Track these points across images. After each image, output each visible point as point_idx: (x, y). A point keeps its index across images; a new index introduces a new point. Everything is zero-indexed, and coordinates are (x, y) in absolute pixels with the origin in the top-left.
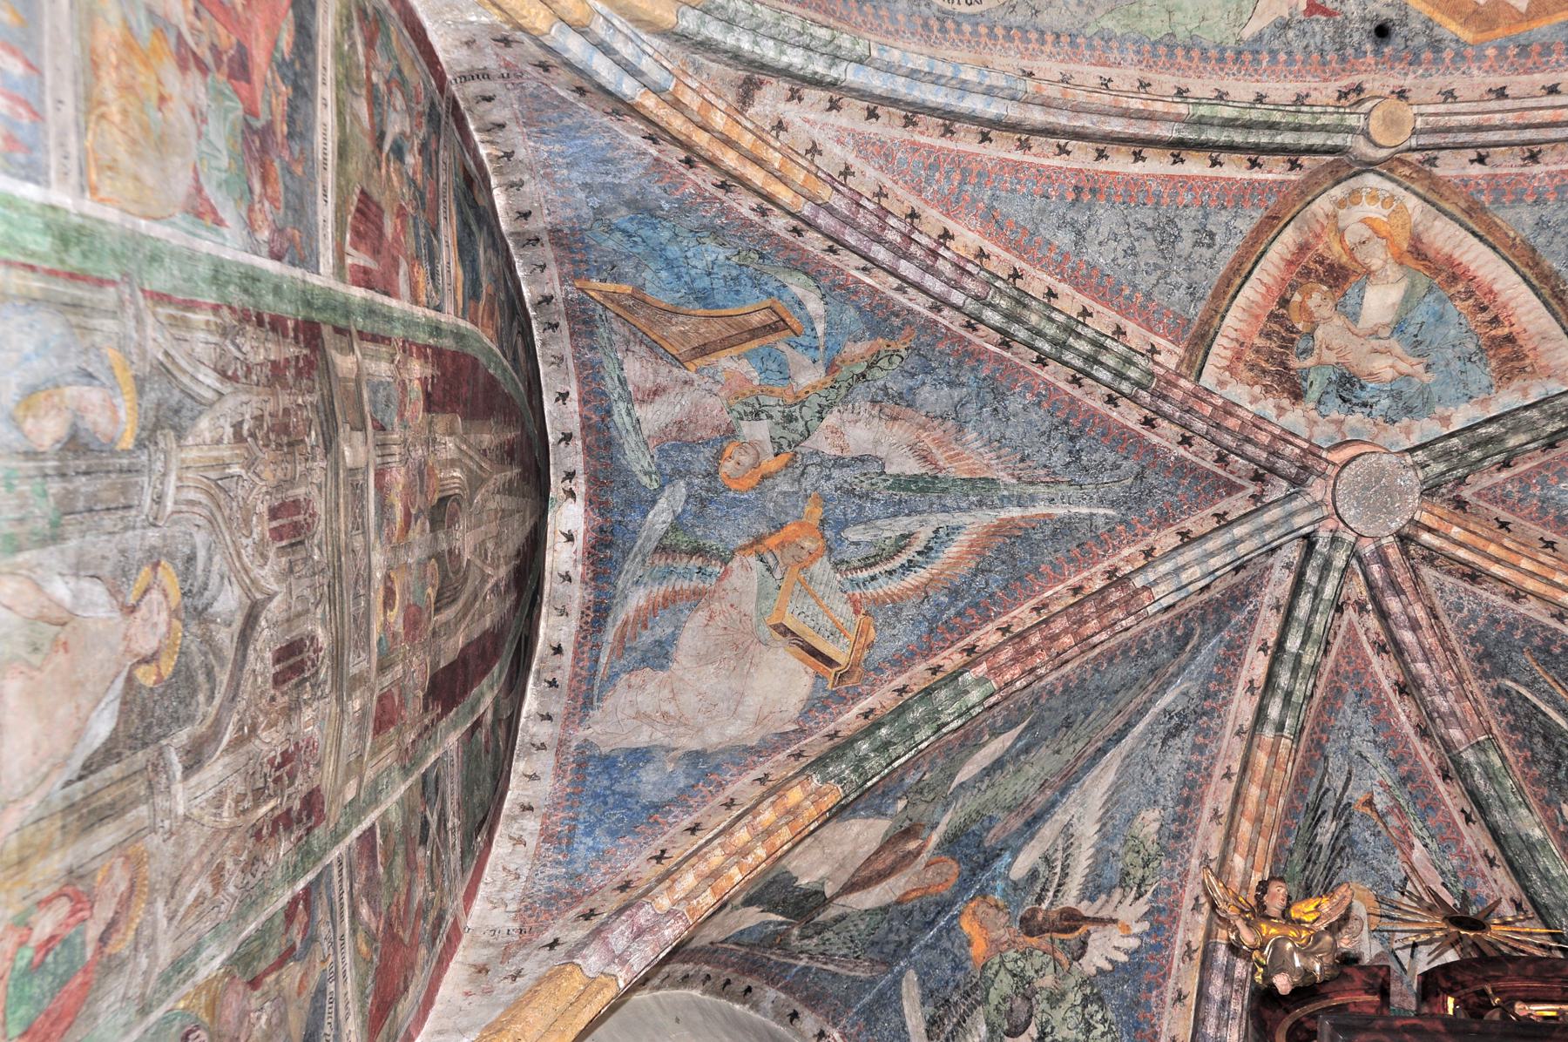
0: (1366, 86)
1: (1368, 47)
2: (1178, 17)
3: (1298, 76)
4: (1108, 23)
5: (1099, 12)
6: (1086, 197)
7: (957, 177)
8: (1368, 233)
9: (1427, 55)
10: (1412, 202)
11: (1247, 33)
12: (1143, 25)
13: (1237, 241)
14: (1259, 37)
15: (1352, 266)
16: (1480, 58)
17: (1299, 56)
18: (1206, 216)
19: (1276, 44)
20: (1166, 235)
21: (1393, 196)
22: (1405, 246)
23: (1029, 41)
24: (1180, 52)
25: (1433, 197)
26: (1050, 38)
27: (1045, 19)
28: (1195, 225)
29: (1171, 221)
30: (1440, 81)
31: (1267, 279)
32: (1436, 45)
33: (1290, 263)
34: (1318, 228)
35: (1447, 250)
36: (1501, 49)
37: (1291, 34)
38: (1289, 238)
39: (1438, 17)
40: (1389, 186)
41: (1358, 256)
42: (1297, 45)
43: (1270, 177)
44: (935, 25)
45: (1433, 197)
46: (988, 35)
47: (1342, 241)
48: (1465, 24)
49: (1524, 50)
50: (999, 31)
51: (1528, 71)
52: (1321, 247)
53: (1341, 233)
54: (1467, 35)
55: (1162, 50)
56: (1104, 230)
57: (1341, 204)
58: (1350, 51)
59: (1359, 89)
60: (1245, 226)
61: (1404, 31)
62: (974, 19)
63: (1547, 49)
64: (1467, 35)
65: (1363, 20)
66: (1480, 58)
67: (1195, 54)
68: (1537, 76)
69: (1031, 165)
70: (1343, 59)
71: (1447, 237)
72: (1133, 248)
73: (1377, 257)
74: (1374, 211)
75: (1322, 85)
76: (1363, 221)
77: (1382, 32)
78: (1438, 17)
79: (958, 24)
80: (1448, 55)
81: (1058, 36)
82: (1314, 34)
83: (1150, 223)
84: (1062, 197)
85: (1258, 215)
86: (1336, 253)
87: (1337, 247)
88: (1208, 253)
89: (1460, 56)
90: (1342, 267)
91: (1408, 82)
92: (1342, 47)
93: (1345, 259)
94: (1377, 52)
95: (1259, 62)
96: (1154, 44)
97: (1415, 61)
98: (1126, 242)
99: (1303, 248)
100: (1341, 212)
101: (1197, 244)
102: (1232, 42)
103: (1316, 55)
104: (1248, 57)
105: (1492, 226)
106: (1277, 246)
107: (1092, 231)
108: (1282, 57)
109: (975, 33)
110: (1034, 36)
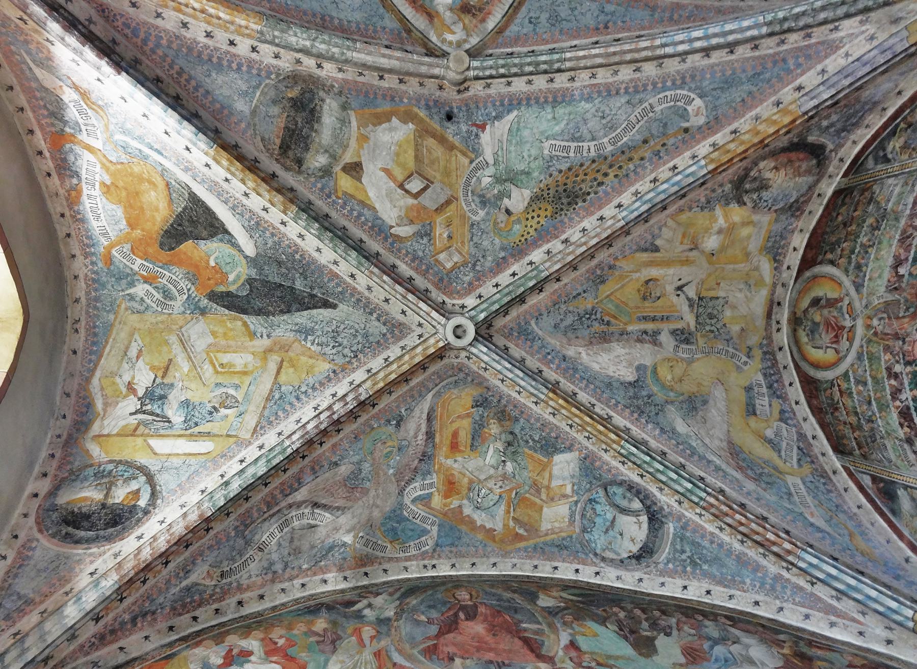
0: (455, 93)
1: (455, 111)
2: (550, 116)
3: (489, 96)
4: (588, 106)
5: (593, 110)
6: (601, 26)
7: (676, 17)
8: (452, 27)
9: (431, 104)
10: (434, 39)
11: (515, 113)
12: (569, 109)
13: (517, 21)
14: (509, 111)
15: (459, 13)
16: (409, 99)
17: (489, 104)
18: (534, 30)
19: (501, 109)
20: (555, 19)
21: (442, 43)
22: (436, 20)
23: (634, 87)
24: (550, 99)
25: (426, 40)
26: (622, 91)
27: (623, 100)
28: (540, 25)
29: (553, 25)
30: (425, 91)
31: (501, 5)
32: (428, 107)
33: (489, 14)
34: (476, 30)
35: (418, 15)
36: (401, 101)
37: (494, 114)
38: (491, 24)
39: (428, 120)
40: (444, 48)
41: (456, 17)
42: (490, 109)
43: (502, 50)
44: (688, 80)
45: (426, 40)
46: (657, 83)
47: (464, 24)
48: (417, 114)
49: (392, 99)
50: (650, 87)
51: (391, 88)
52: (474, 21)
53: (465, 28)
54: (416, 109)
55: (559, 99)
56: (589, 15)
57: (465, 41)
58: (464, 109)
59: (459, 92)
60: (513, 29)
61: (441, 116)
62: (664, 89)
63: (384, 97)
64: (416, 109)
65: (458, 122)
66: (409, 99)
67: (542, 100)
68: (387, 86)
69: (635, 31)
70: (467, 105)
71: (418, 21)
72: (572, 11)
73: (448, 16)
74: (449, 37)
75: (478, 93)
76: (454, 33)
77: (449, 117)
78: (428, 120)
79: (673, 84)
80: (423, 102)
81: (617, 93)
82: (482, 115)
83: (564, 22)
84: (615, 23)
85: (507, 33)
86: (467, 19)
87: (467, 21)
88: (532, 14)
89: (418, 101)
90: (463, 12)
91: (438, 93)
92: (468, 111)
93: (463, 16)
94: (452, 108)
95: (509, 100)
96: (563, 101)
97: (436, 102)
98: (576, 13)
99: (483, 20)
100: (464, 37)
101: (539, 18)
102: (523, 108)
103: (481, 105)
104: (515, 102)
105: (401, 21)
106: (497, 20)
107: (595, 15)
108: (498, 103)
109: (664, 82)
110: (631, 90)
